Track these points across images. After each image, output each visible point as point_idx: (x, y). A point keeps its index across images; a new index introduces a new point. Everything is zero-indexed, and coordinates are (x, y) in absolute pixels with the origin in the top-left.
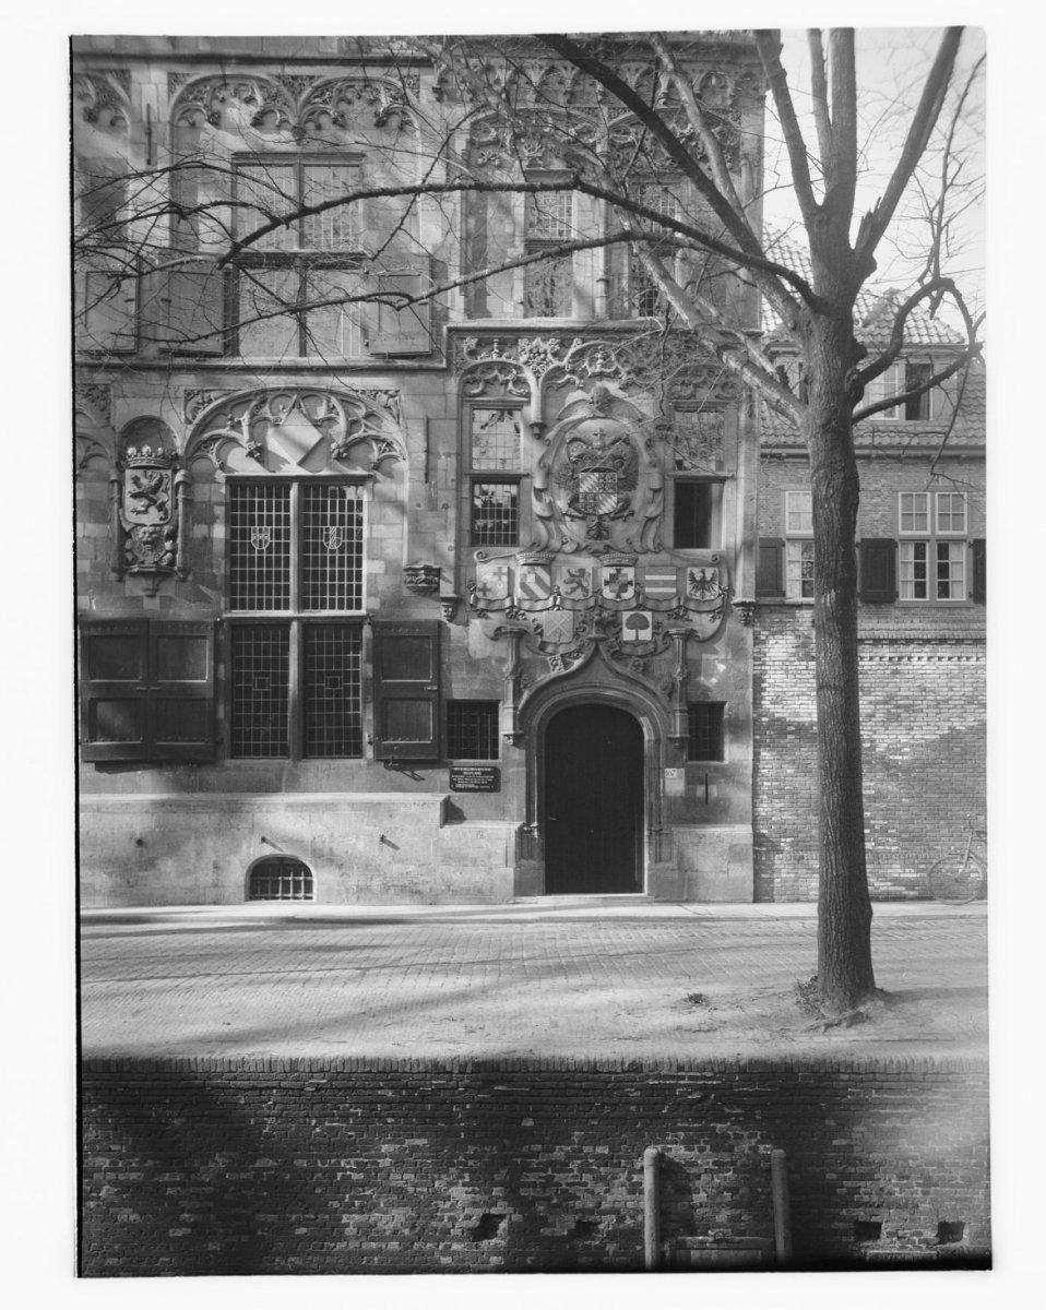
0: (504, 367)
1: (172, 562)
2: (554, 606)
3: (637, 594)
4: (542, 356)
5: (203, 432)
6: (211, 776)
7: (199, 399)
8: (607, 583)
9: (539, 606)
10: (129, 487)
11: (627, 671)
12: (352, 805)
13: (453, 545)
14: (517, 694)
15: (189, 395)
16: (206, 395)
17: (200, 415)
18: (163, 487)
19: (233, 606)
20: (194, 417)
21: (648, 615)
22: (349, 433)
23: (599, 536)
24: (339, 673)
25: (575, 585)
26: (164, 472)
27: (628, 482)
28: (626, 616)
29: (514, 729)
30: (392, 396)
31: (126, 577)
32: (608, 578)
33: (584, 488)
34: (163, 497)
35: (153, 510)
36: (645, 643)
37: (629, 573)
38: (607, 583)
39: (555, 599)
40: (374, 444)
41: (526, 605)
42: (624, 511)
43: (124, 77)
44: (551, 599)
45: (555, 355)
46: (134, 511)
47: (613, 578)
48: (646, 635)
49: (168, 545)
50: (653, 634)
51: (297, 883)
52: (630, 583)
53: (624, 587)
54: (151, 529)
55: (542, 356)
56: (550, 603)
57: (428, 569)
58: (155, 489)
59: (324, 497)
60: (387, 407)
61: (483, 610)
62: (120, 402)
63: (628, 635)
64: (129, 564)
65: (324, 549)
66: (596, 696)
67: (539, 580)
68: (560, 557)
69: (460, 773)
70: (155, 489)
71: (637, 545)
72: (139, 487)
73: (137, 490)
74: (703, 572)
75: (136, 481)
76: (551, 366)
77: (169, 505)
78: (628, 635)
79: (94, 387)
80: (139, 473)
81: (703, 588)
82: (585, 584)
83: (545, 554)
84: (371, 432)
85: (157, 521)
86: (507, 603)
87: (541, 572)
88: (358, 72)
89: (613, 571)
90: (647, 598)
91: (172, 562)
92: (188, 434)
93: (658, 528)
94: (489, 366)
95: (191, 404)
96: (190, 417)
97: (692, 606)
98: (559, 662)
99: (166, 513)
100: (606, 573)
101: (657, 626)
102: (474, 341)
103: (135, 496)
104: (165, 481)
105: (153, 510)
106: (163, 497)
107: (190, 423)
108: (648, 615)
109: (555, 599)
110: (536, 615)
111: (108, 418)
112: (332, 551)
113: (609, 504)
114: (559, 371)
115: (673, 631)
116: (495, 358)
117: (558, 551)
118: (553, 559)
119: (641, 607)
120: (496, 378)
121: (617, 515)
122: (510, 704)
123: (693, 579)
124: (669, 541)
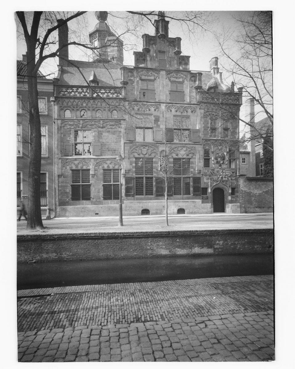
6: (172, 197)
11: (224, 184)
12: (190, 201)
15: (169, 147)
21: (226, 176)
23: (220, 166)
27: (224, 159)
28: (224, 176)
33: (219, 160)
37: (224, 171)
42: (223, 163)
43: (160, 105)
47: (222, 172)
48: (226, 179)
59: (188, 162)
78: (224, 179)
88: (190, 105)
100: (221, 171)
108: (226, 176)
113: (222, 162)
121: (222, 164)
122: (210, 188)
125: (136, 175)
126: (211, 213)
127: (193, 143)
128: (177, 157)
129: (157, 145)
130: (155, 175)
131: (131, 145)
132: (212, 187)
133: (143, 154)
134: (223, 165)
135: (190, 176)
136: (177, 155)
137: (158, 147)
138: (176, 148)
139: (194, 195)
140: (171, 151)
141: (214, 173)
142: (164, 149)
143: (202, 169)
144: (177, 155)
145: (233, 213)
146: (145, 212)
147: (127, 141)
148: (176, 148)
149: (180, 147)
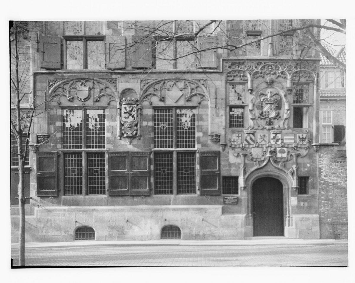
0: (239, 72)
1: (136, 134)
2: (256, 146)
3: (282, 143)
4: (252, 68)
5: (146, 93)
6: (149, 200)
7: (144, 82)
8: (272, 139)
9: (251, 146)
10: (123, 110)
11: (279, 166)
12: (193, 209)
13: (224, 127)
14: (245, 173)
16: (147, 81)
17: (145, 88)
18: (134, 110)
19: (155, 147)
20: (143, 88)
21: (285, 149)
22: (191, 93)
23: (270, 124)
24: (75, 168)
26: (134, 106)
29: (244, 185)
30: (205, 81)
31: (122, 138)
32: (273, 138)
34: (133, 113)
35: (130, 117)
36: (285, 158)
37: (279, 136)
38: (272, 139)
39: (256, 144)
40: (199, 96)
41: (247, 146)
42: (278, 117)
44: (255, 144)
45: (256, 67)
46: (125, 118)
47: (274, 138)
48: (285, 155)
49: (135, 128)
51: (176, 233)
52: (280, 139)
53: (277, 140)
54: (130, 123)
55: (252, 68)
56: (255, 146)
57: (216, 135)
58: (131, 111)
60: (203, 85)
61: (233, 148)
62: (120, 84)
63: (279, 155)
64: (123, 134)
65: (183, 129)
66: (268, 175)
67: (251, 139)
68: (258, 131)
69: (226, 199)
70: (131, 111)
71: (281, 126)
72: (126, 110)
73: (126, 111)
74: (303, 135)
75: (125, 108)
76: (255, 71)
77: (135, 116)
78: (279, 155)
79: (112, 79)
80: (126, 106)
81: (303, 140)
82: (265, 139)
83: (253, 130)
84: (198, 92)
85: (132, 121)
86: (241, 146)
87: (251, 135)
89: (274, 135)
90: (285, 144)
91: (136, 134)
92: (141, 94)
93: (288, 122)
94: (235, 71)
95: (142, 84)
96: (142, 88)
97: (299, 146)
98: (258, 164)
99: (135, 118)
100: (272, 136)
101: (288, 152)
102: (230, 63)
103: (125, 113)
104: (134, 108)
105: (130, 117)
106: (133, 113)
107: (142, 90)
108: (285, 149)
109: (256, 144)
111: (117, 89)
112: (186, 130)
113: (273, 114)
114: (257, 72)
115: (293, 154)
116: (237, 69)
117: (257, 129)
118: (255, 132)
119: (282, 146)
120: (237, 75)
123: (299, 137)
124: (292, 126)
125: (64, 147)
126: (246, 236)
127: (201, 70)
128: (161, 104)
129: (114, 76)
130: (108, 147)
131: (52, 78)
132: (248, 174)
133: (80, 100)
134: (276, 121)
135: (196, 149)
136: (162, 99)
137: (114, 82)
138: (158, 82)
139: (202, 194)
140: (146, 91)
141: (253, 141)
142: (129, 86)
143: (222, 133)
144: (161, 100)
145: (301, 238)
146: (84, 232)
147: (42, 68)
148: (158, 82)
149: (170, 80)
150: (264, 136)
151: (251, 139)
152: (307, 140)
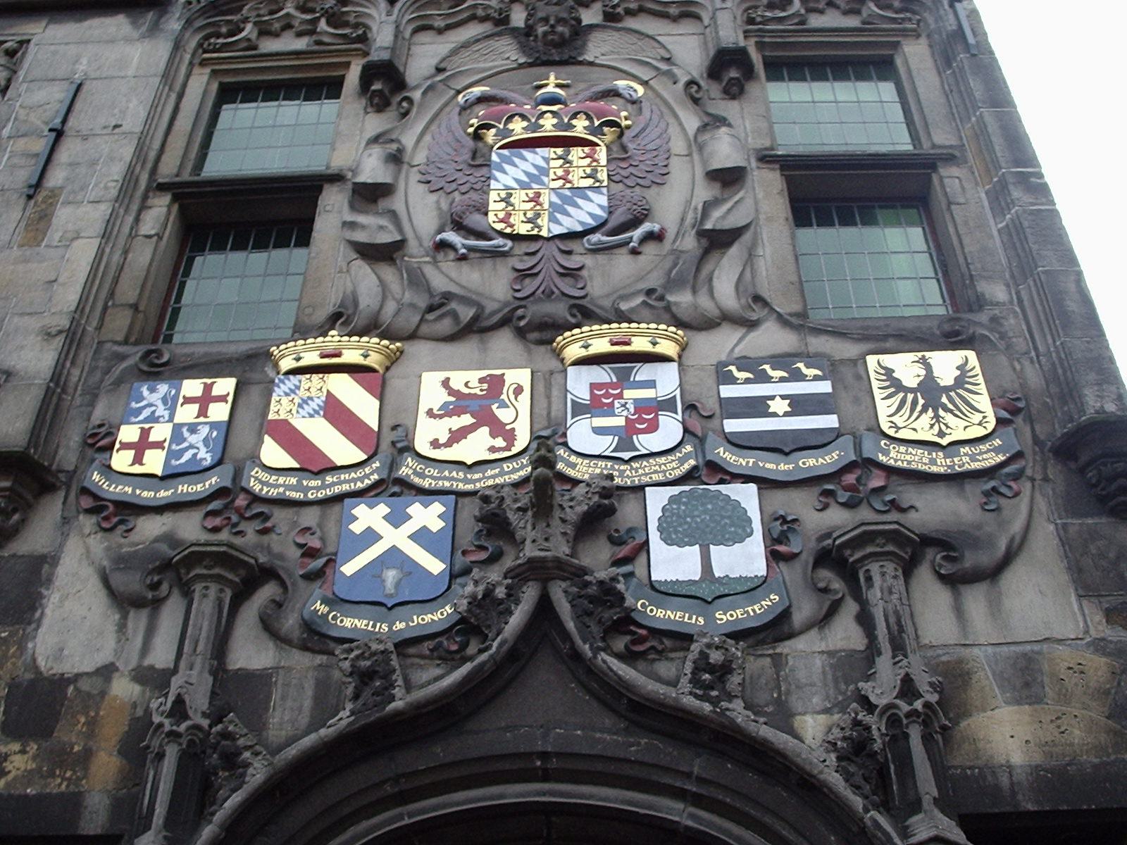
25: (467, 420)
36: (752, 589)
50: (774, 556)
56: (371, 474)
63: (672, 563)
67: (336, 412)
74: (924, 362)
78: (672, 563)
82: (504, 415)
86: (213, 481)
87: (345, 388)
89: (602, 374)
110: (309, 517)
117: (413, 336)
118: (393, 359)
123: (896, 385)
150: (495, 384)
151: (336, 412)
152: (983, 401)
